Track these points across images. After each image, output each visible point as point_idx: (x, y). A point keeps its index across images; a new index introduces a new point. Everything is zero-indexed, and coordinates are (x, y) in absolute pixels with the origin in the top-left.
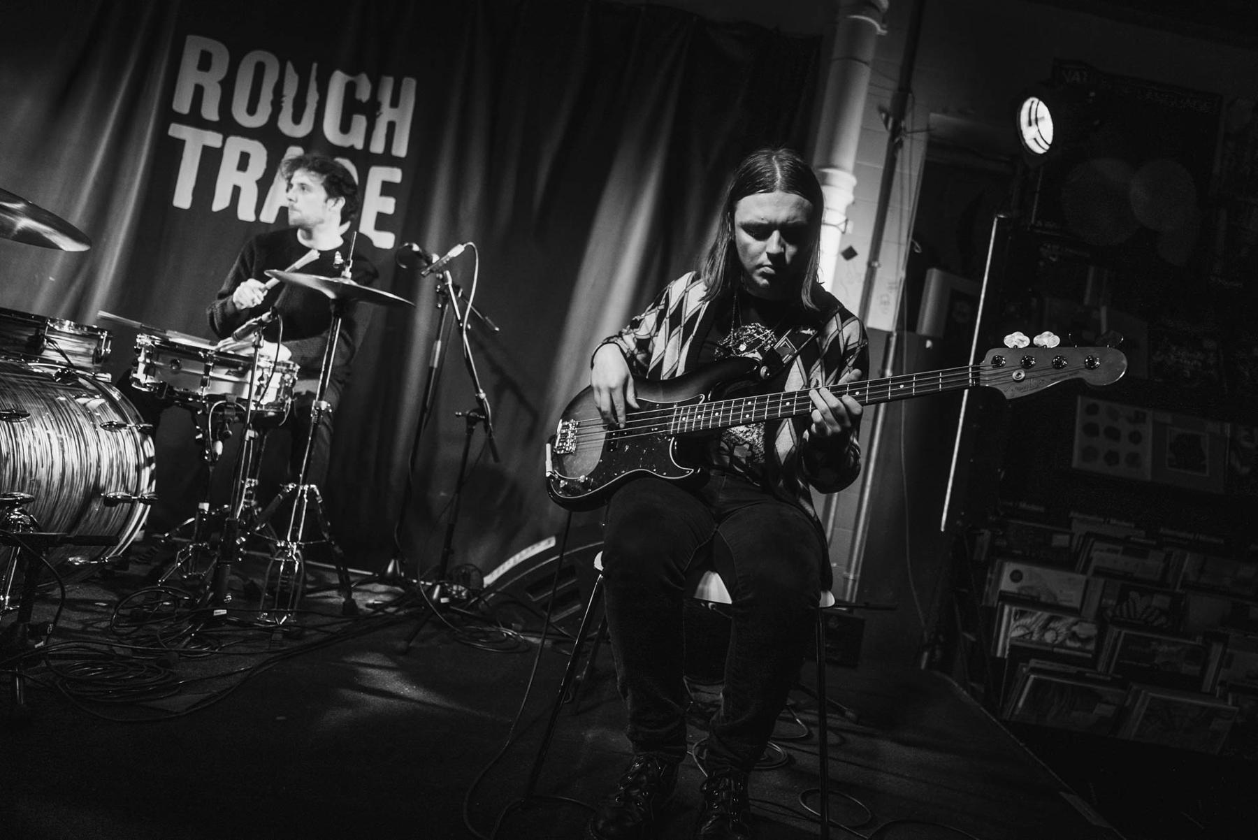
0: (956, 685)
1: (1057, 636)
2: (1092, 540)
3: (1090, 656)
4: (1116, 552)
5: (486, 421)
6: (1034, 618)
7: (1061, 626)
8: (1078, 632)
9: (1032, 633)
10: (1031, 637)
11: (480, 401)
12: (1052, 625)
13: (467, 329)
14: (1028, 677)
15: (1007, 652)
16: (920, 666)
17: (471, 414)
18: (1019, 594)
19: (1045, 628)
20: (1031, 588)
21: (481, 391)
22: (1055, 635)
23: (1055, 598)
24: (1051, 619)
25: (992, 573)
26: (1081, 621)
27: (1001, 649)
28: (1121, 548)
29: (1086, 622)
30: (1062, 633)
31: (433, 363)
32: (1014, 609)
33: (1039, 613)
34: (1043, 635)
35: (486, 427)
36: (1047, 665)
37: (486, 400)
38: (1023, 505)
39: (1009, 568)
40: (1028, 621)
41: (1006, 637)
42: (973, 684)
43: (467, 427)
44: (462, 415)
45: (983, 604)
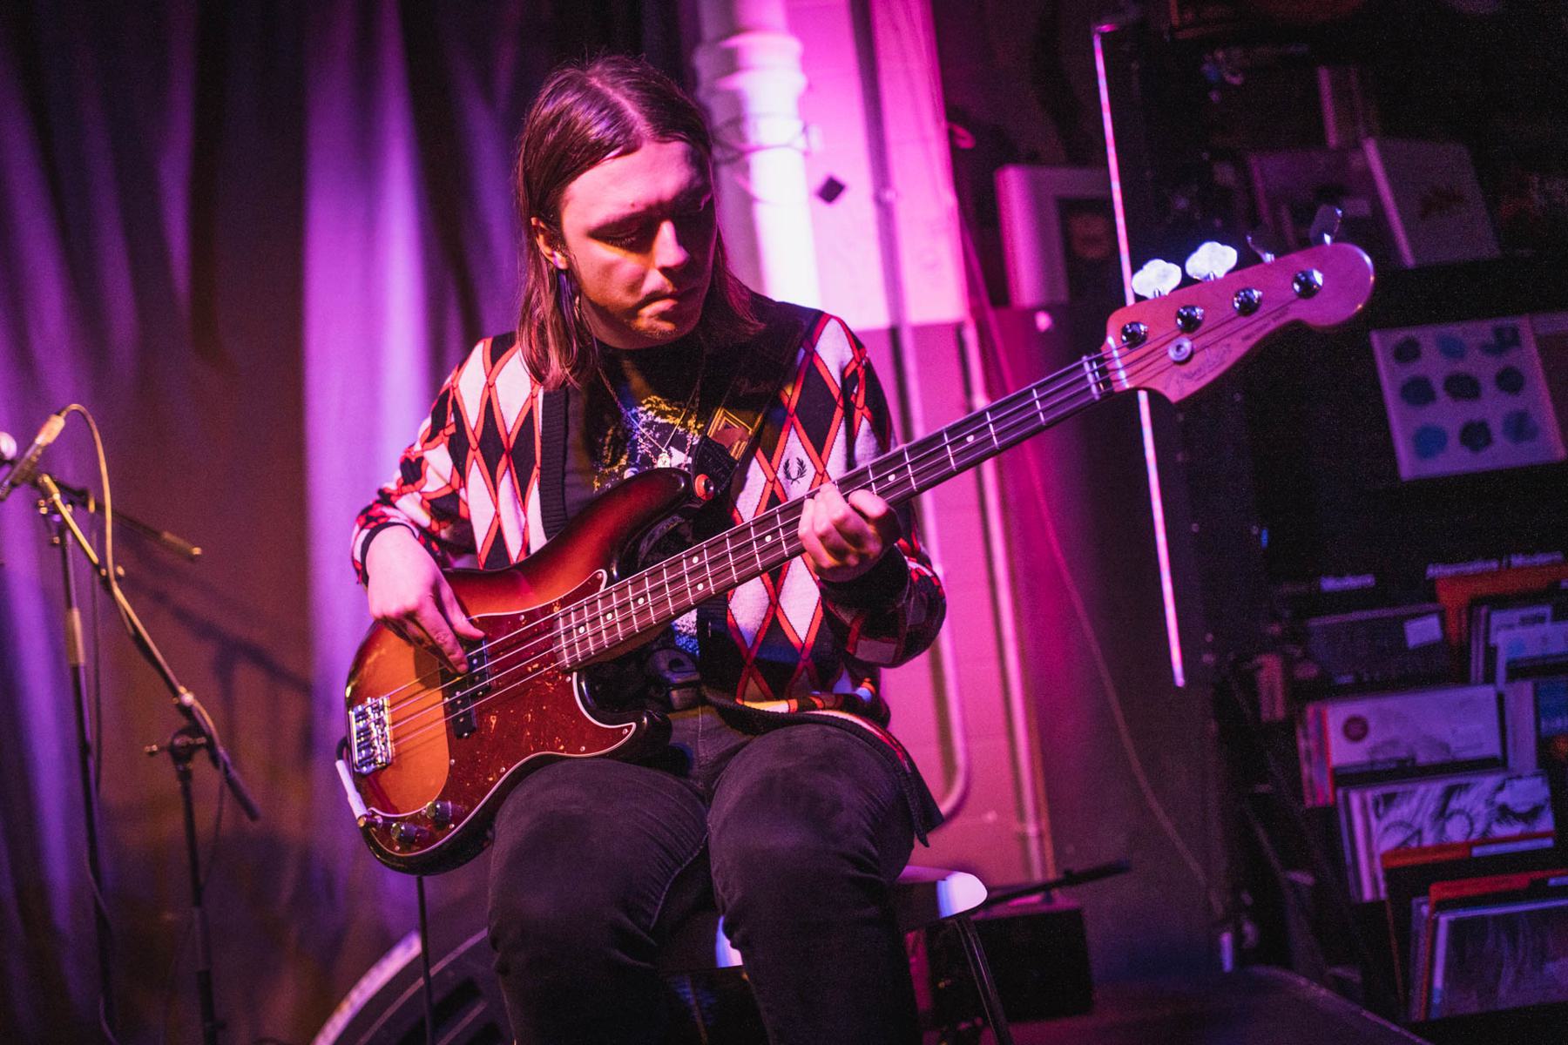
0: (1303, 981)
1: (1471, 824)
2: (1484, 610)
3: (1549, 843)
4: (1540, 619)
5: (210, 746)
6: (1415, 802)
7: (1476, 798)
8: (1510, 803)
9: (1419, 832)
10: (1420, 840)
11: (187, 711)
12: (1454, 804)
13: (118, 578)
14: (1436, 922)
15: (1382, 886)
16: (1221, 966)
17: (177, 742)
18: (1372, 763)
19: (1442, 814)
20: (1393, 743)
21: (182, 690)
22: (1467, 822)
23: (1446, 747)
24: (1449, 793)
25: (1306, 736)
26: (1510, 779)
27: (1369, 885)
28: (1547, 610)
29: (1519, 777)
30: (1478, 814)
31: (76, 659)
32: (1370, 795)
33: (1422, 789)
34: (1443, 830)
35: (214, 758)
36: (1470, 889)
37: (197, 705)
38: (1329, 584)
39: (1337, 716)
40: (1402, 811)
41: (1371, 856)
42: (1339, 971)
43: (178, 770)
44: (161, 749)
45: (1309, 803)
